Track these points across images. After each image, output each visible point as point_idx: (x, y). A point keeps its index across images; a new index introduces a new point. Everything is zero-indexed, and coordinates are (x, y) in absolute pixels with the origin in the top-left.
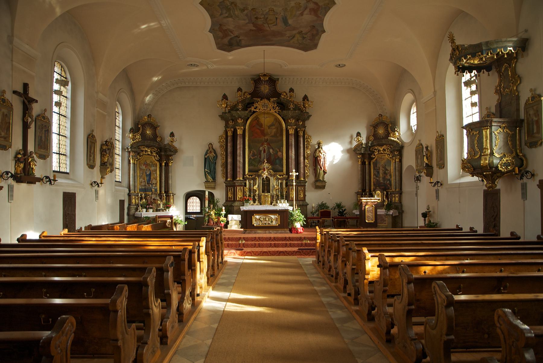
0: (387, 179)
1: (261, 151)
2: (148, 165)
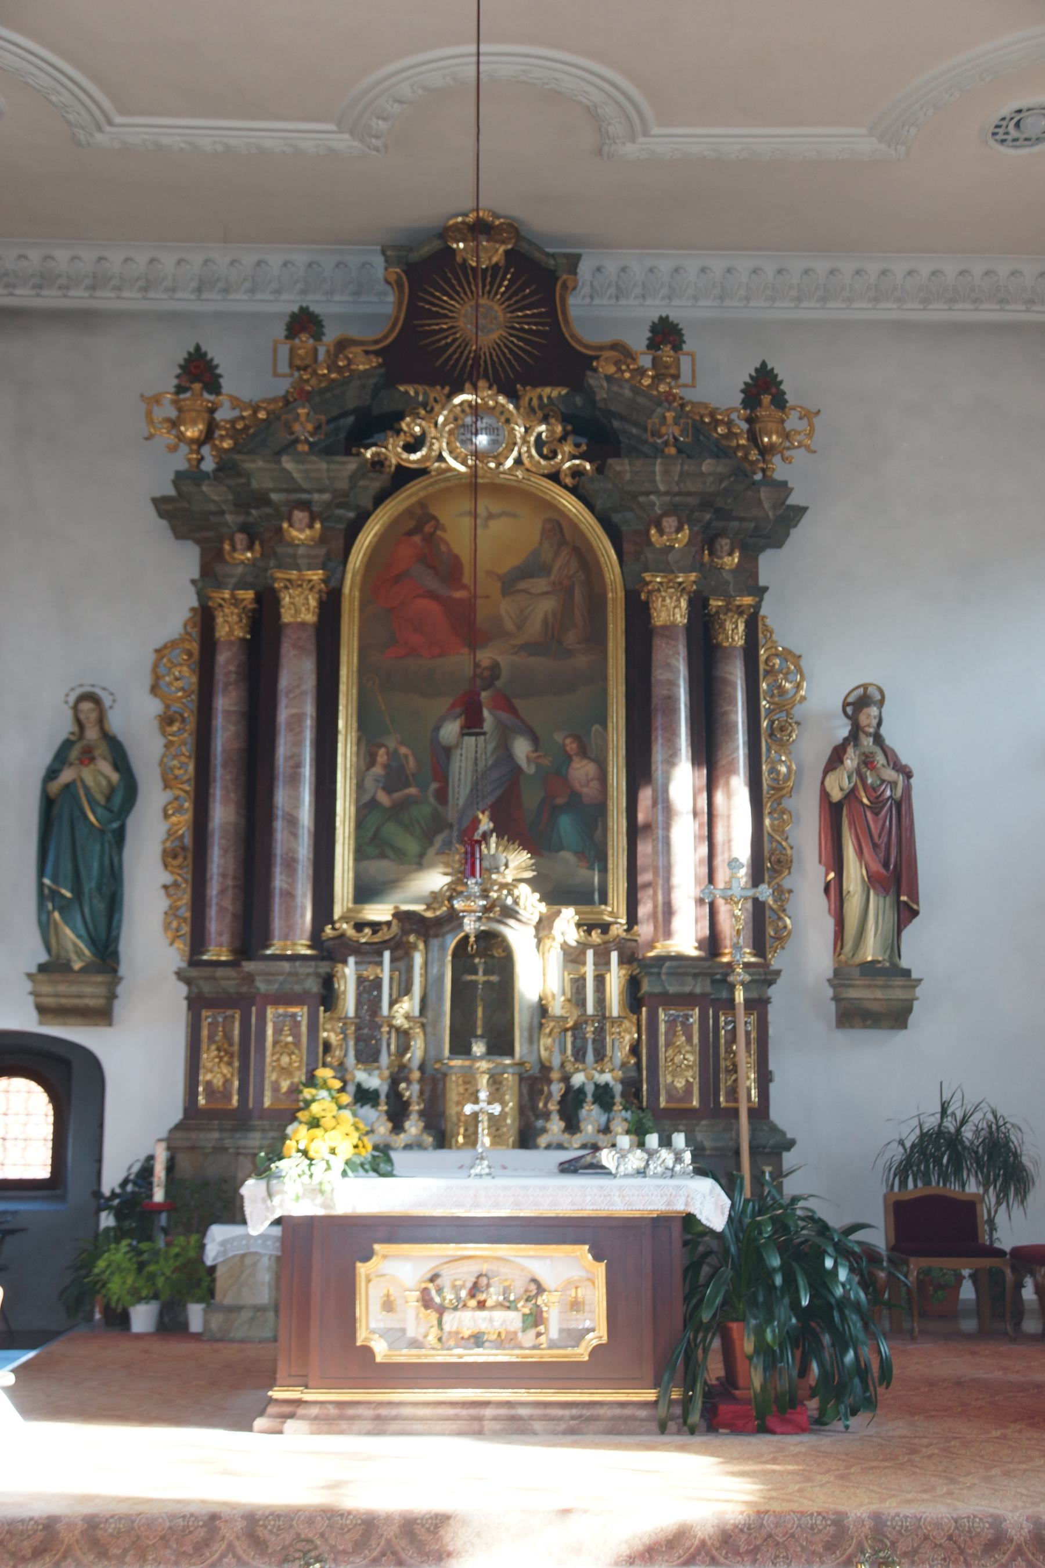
1: (448, 751)
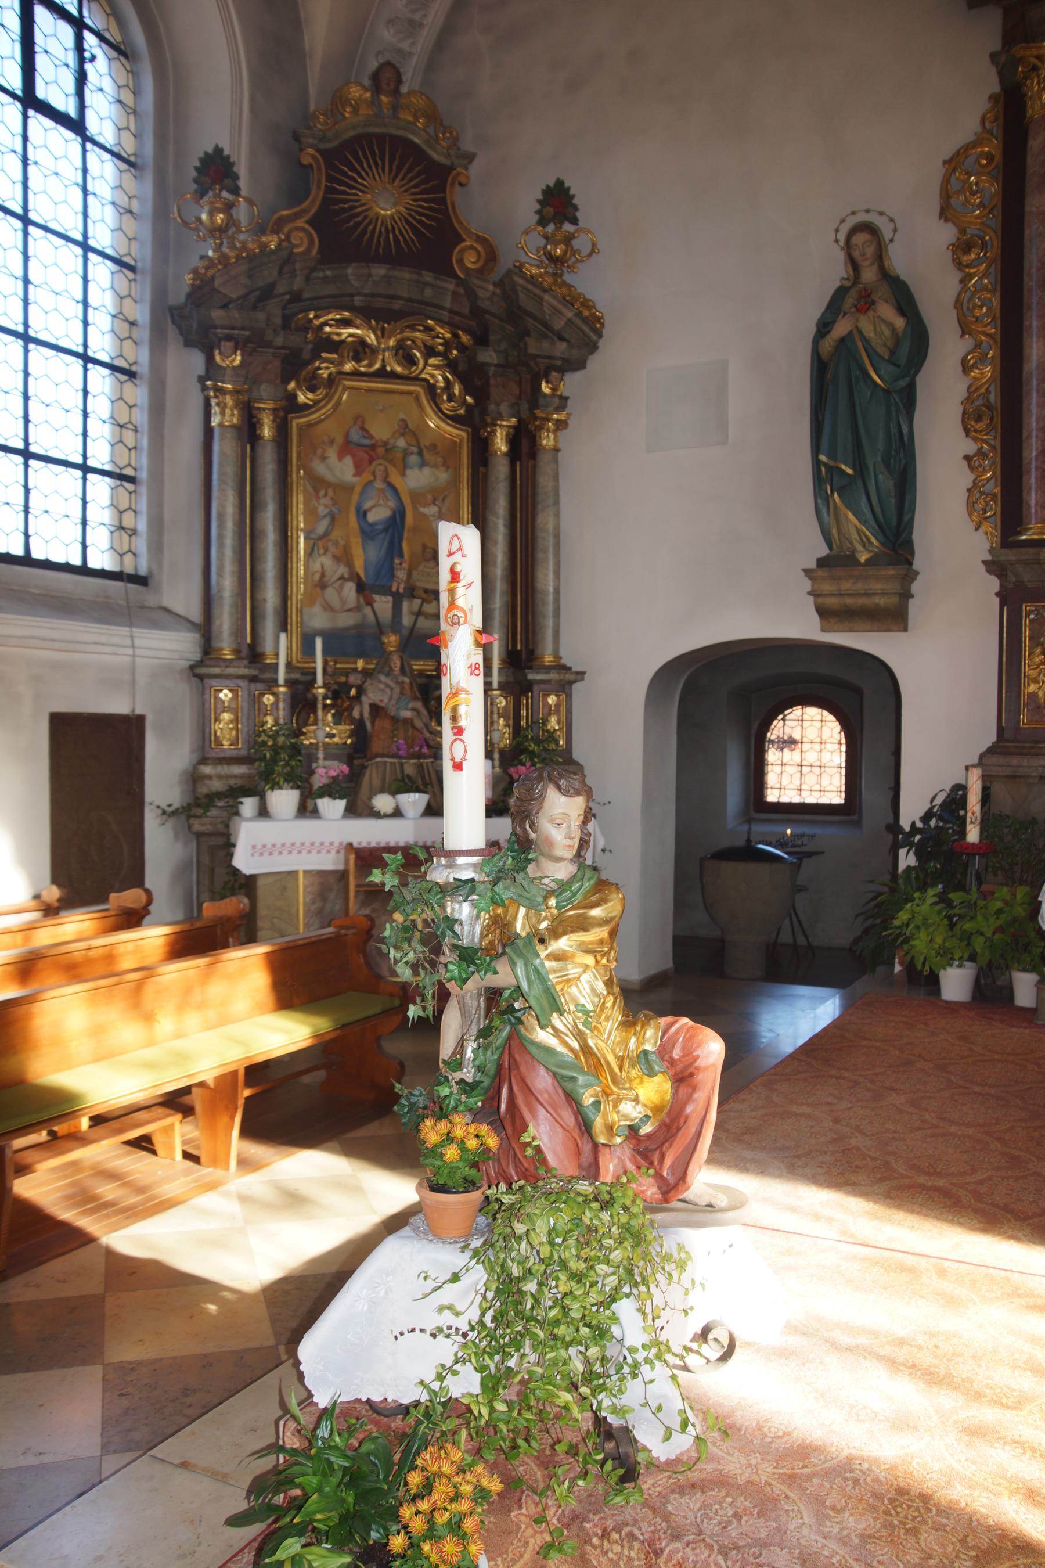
2: (381, 450)
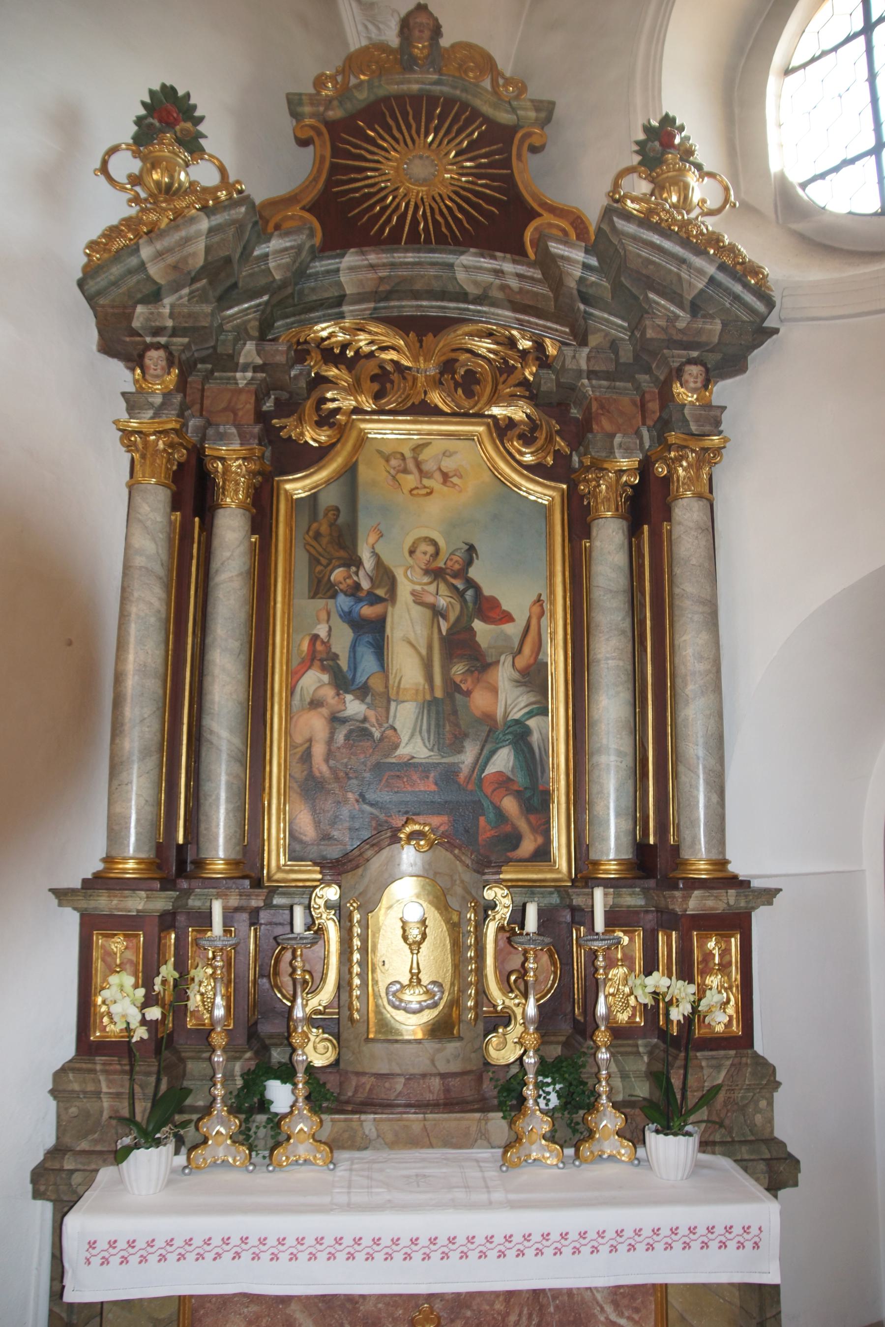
0: (488, 718)
